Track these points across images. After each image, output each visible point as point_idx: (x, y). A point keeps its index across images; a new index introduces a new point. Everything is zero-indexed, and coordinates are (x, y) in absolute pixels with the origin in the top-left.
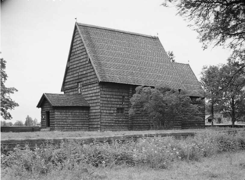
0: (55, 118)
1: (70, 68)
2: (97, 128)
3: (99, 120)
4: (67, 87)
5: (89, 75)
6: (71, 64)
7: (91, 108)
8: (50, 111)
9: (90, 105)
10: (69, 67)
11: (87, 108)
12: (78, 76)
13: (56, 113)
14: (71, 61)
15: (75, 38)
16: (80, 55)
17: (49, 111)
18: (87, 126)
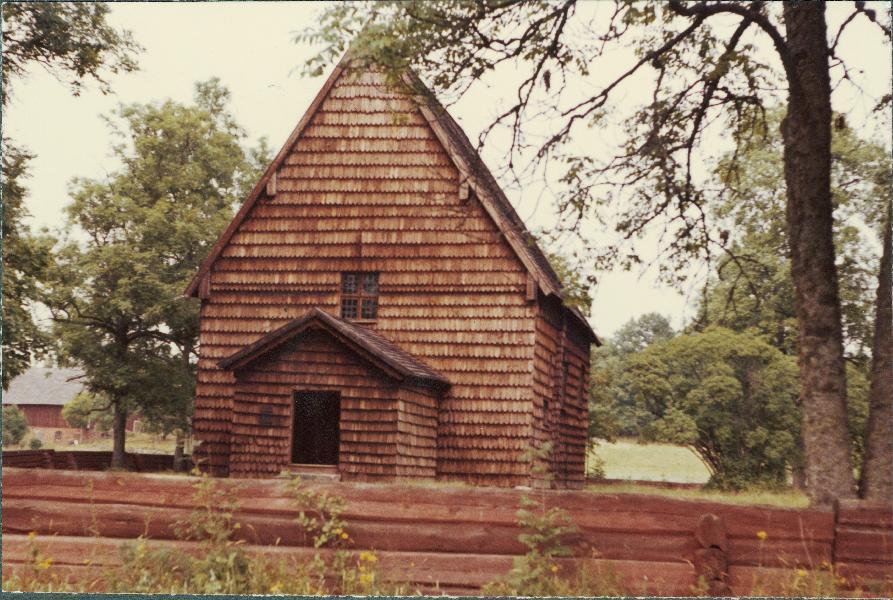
0: (401, 427)
1: (286, 199)
2: (509, 476)
3: (523, 444)
4: (233, 278)
5: (446, 252)
6: (289, 186)
7: (457, 392)
8: (344, 393)
9: (454, 379)
10: (273, 197)
11: (439, 389)
12: (358, 245)
13: (401, 406)
14: (286, 173)
15: (342, 81)
16: (384, 160)
17: (339, 392)
18: (434, 464)
